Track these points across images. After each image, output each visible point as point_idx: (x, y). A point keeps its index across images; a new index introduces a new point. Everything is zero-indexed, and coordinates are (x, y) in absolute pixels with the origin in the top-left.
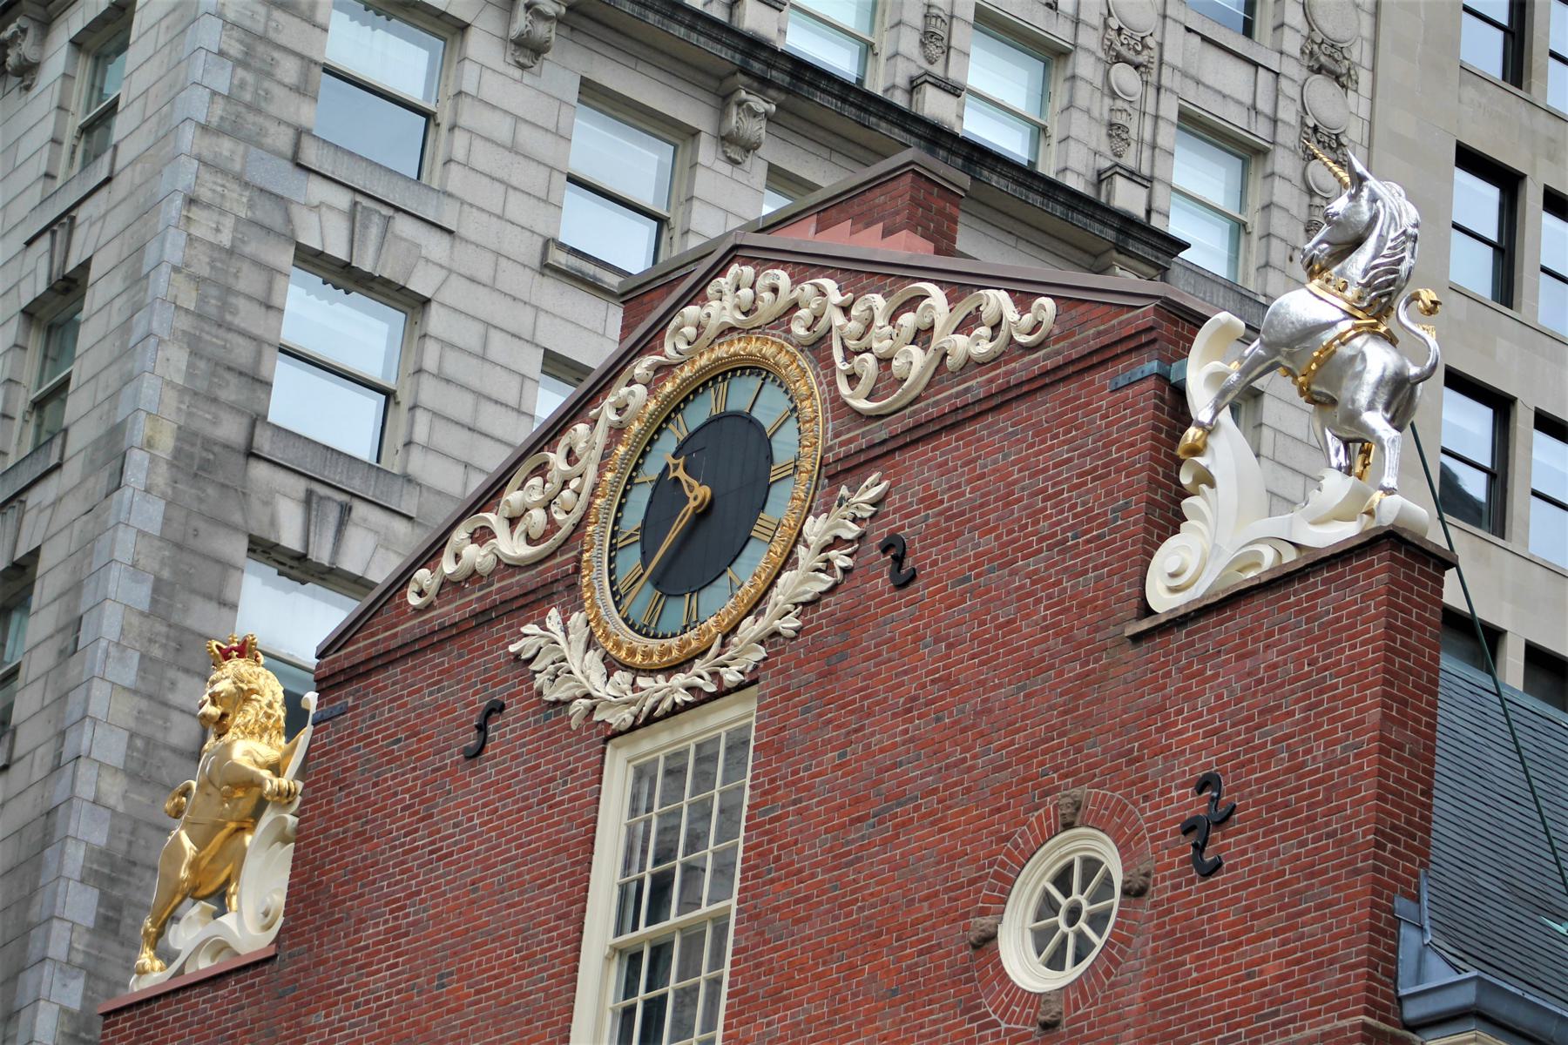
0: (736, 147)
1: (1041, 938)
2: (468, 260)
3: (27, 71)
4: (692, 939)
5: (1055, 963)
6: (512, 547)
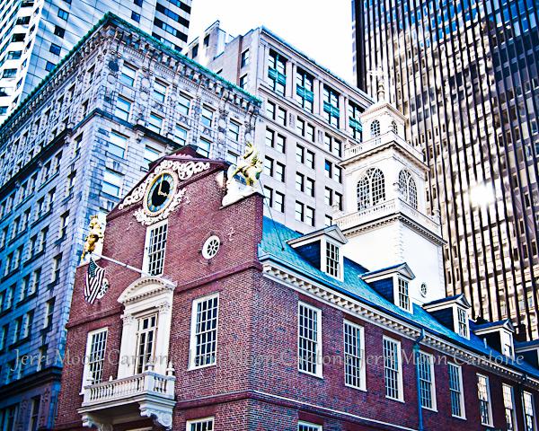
3: (68, 143)
6: (133, 201)
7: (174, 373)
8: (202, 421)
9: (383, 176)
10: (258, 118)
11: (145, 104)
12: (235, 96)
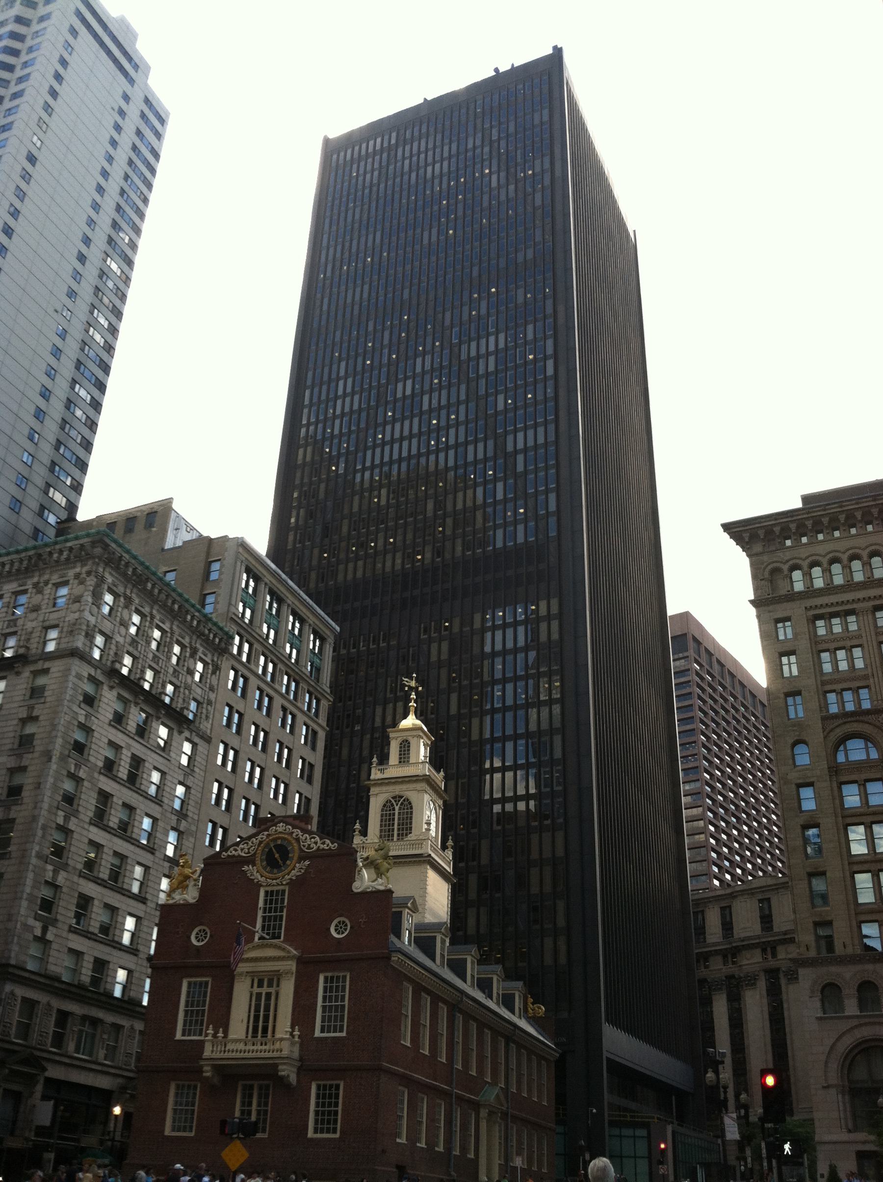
0: (136, 704)
1: (336, 930)
2: (100, 723)
4: (276, 917)
5: (338, 933)
7: (299, 1037)
8: (329, 1083)
9: (411, 808)
10: (226, 655)
11: (121, 640)
12: (210, 630)
